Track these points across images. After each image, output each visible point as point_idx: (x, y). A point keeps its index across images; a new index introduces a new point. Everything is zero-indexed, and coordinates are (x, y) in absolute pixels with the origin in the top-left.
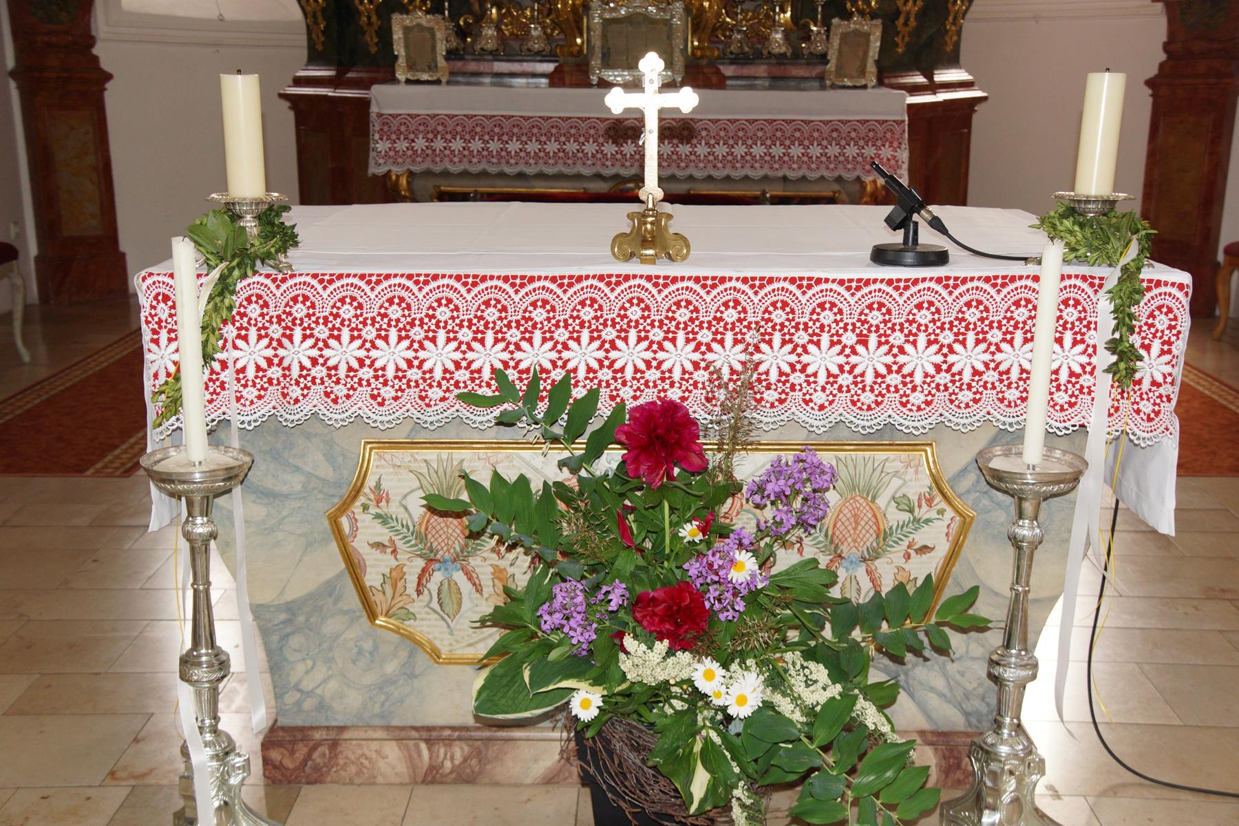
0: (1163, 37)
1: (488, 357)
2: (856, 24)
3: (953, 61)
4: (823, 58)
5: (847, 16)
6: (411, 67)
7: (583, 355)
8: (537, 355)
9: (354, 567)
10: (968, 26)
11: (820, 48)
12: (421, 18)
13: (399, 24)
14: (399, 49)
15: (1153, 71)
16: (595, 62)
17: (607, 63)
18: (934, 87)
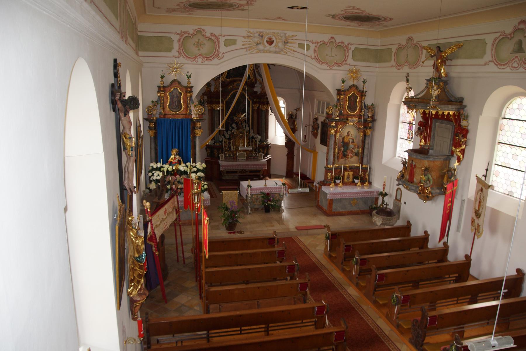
0: (287, 151)
1: (260, 191)
2: (261, 153)
3: (269, 154)
4: (258, 156)
5: (260, 153)
6: (221, 159)
7: (264, 191)
8: (262, 191)
9: (253, 200)
10: (270, 151)
11: (257, 155)
12: (222, 154)
13: (220, 155)
14: (220, 157)
15: (287, 154)
16: (238, 158)
17: (239, 157)
18: (267, 158)
